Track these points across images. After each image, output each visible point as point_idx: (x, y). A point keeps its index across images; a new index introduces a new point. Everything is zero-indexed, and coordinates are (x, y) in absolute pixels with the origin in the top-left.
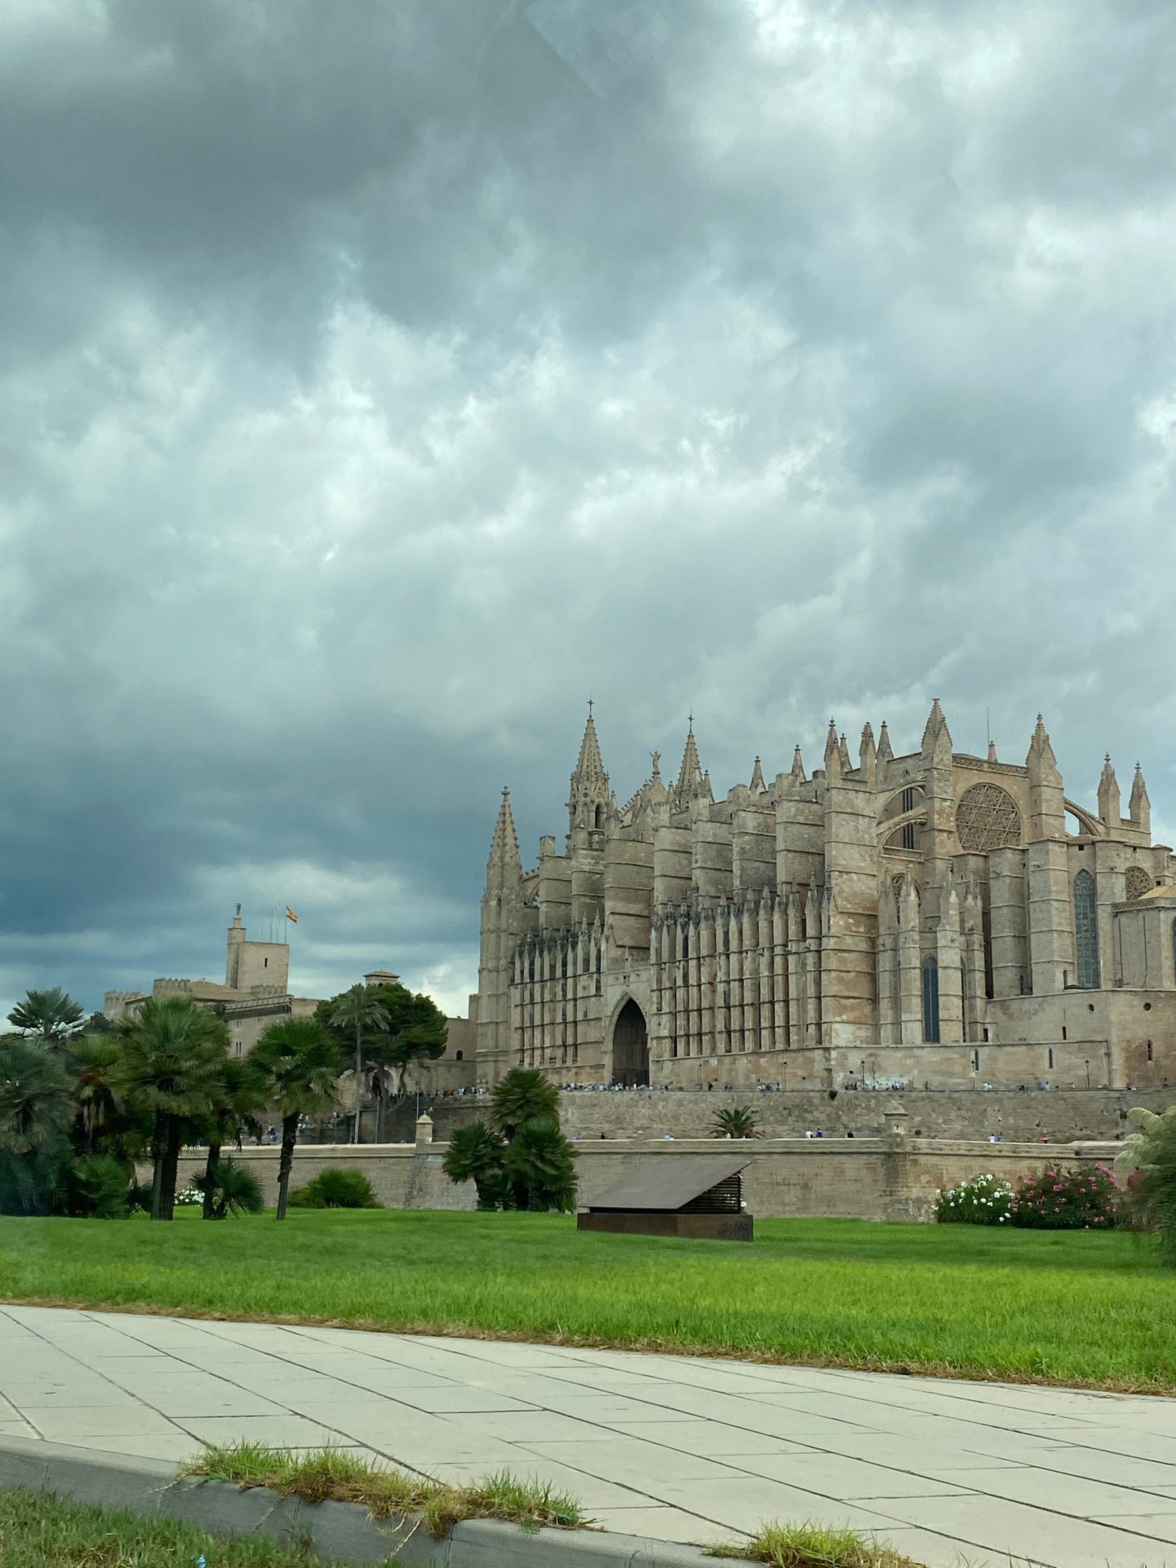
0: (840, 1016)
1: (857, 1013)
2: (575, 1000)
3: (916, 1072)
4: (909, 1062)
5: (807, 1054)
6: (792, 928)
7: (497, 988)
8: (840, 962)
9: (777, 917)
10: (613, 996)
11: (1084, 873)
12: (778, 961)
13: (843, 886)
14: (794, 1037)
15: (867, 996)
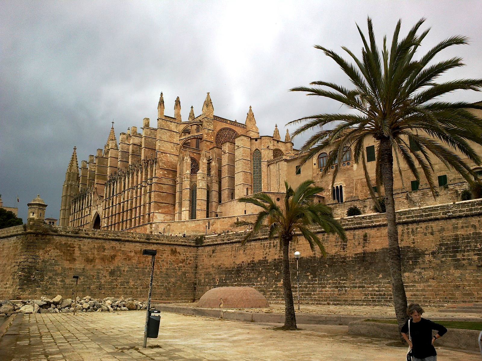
0: (158, 210)
1: (166, 210)
2: (84, 217)
3: (185, 231)
4: (183, 227)
5: (145, 226)
6: (144, 177)
7: (65, 216)
8: (159, 188)
9: (139, 174)
10: (93, 213)
11: (257, 151)
12: (139, 190)
13: (162, 158)
14: (142, 220)
15: (171, 203)
